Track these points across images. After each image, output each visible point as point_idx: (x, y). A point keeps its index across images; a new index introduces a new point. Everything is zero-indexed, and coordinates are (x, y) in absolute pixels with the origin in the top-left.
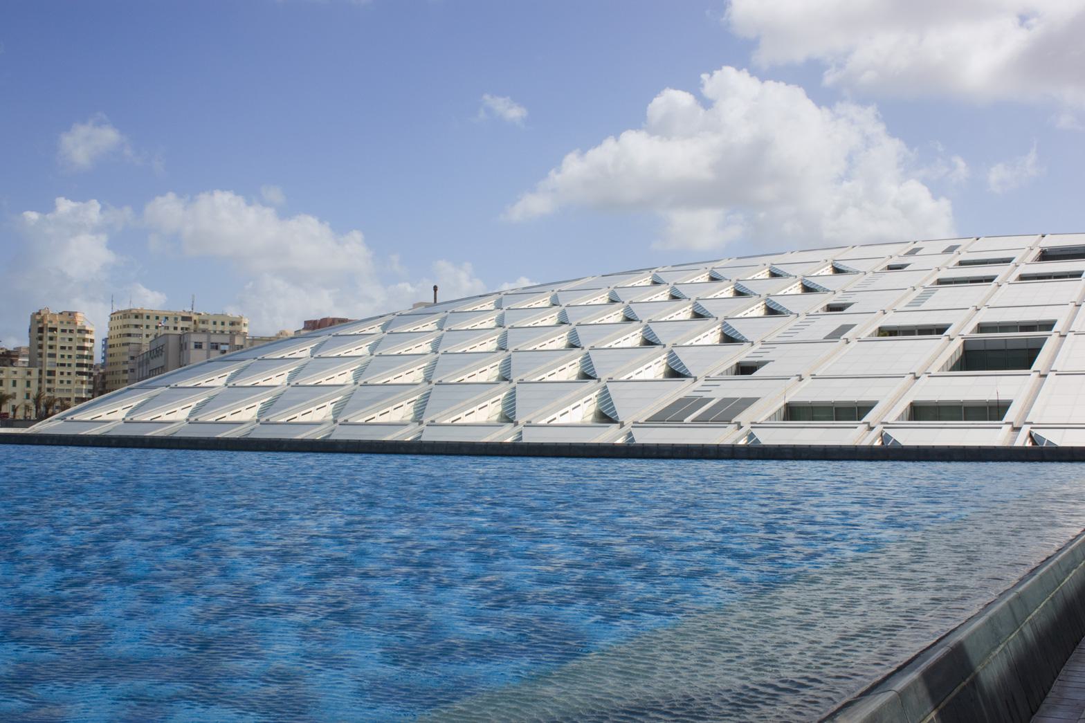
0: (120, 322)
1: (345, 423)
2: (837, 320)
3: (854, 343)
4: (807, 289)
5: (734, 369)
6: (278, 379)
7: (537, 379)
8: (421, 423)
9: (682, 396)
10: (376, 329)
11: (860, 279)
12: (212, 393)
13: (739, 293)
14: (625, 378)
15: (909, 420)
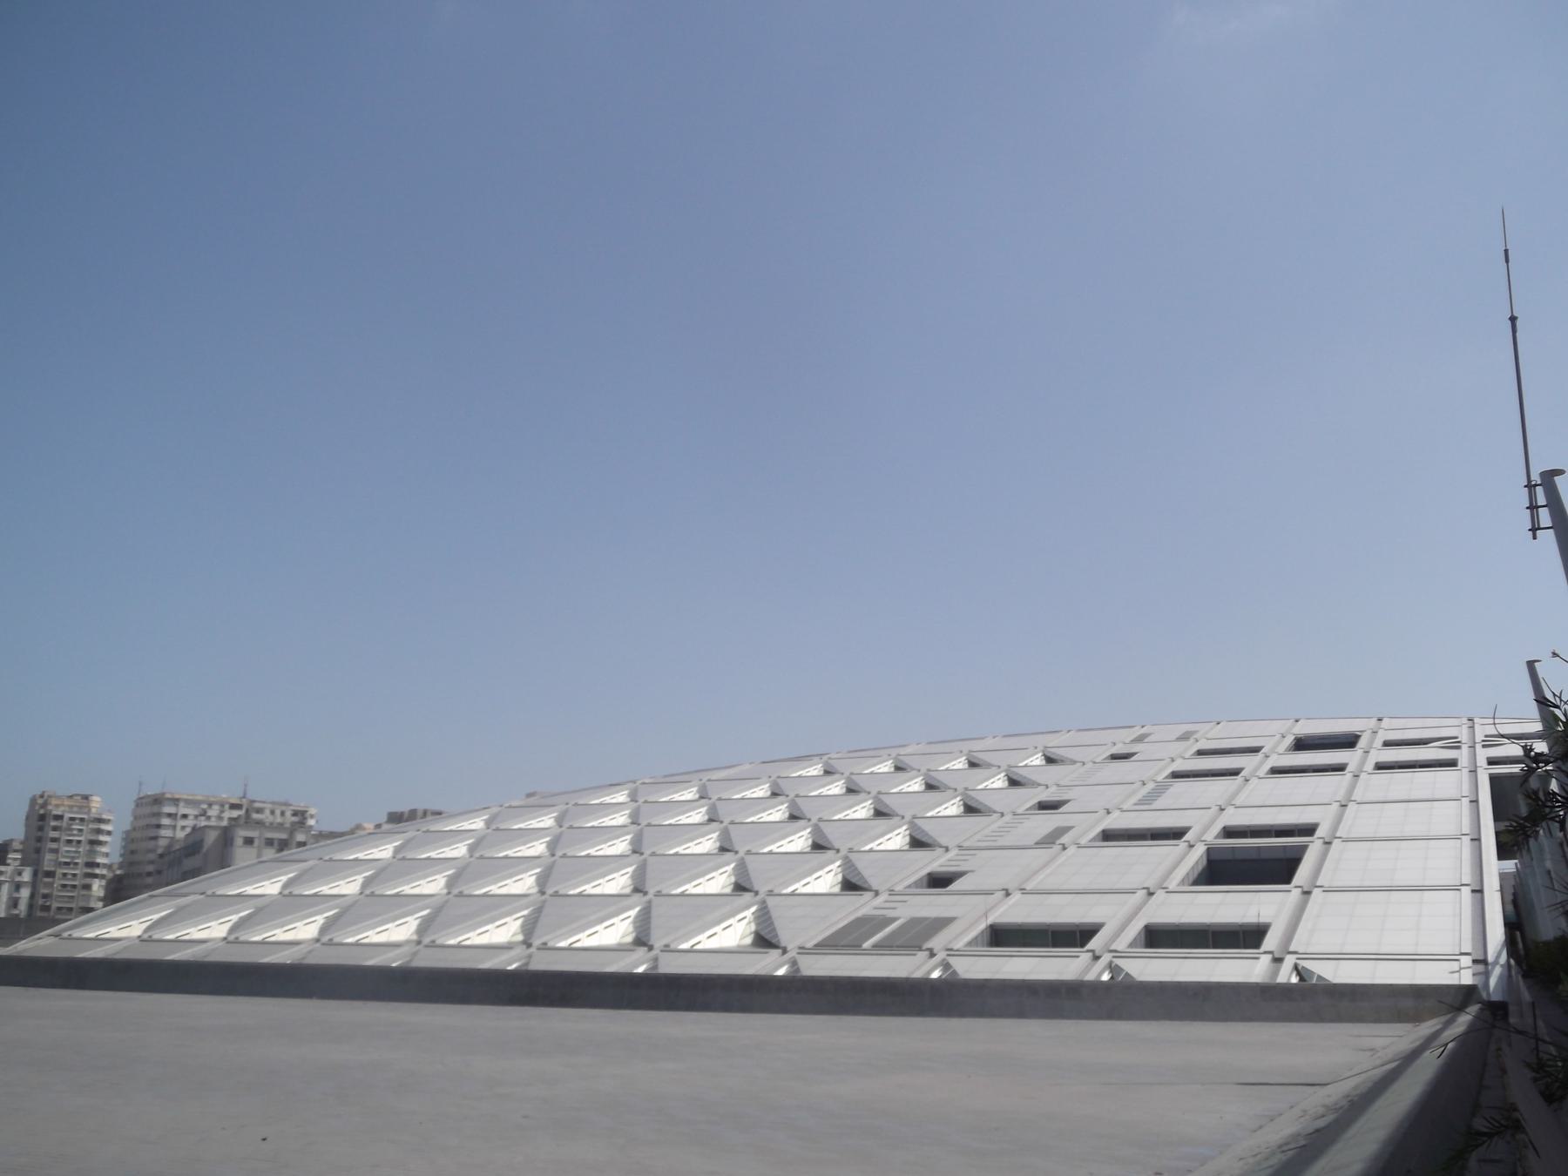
0: (147, 810)
1: (433, 945)
2: (1050, 821)
5: (925, 882)
6: (349, 886)
9: (859, 914)
10: (477, 824)
12: (259, 902)
14: (789, 890)
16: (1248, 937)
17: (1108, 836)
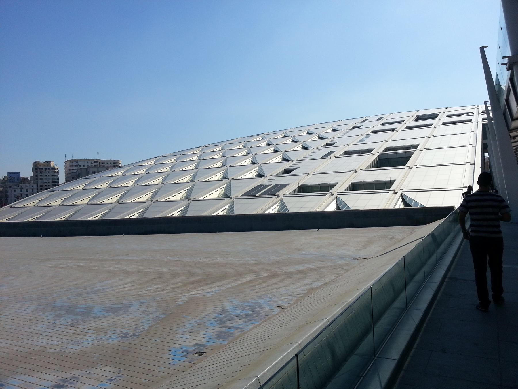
0: (68, 165)
3: (333, 158)
4: (320, 138)
7: (205, 180)
8: (152, 201)
11: (342, 132)
13: (293, 141)
15: (350, 190)
16: (386, 185)
17: (346, 153)
